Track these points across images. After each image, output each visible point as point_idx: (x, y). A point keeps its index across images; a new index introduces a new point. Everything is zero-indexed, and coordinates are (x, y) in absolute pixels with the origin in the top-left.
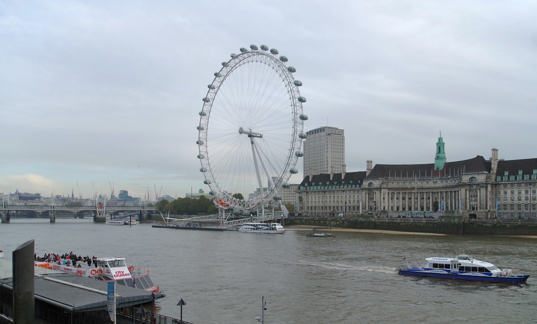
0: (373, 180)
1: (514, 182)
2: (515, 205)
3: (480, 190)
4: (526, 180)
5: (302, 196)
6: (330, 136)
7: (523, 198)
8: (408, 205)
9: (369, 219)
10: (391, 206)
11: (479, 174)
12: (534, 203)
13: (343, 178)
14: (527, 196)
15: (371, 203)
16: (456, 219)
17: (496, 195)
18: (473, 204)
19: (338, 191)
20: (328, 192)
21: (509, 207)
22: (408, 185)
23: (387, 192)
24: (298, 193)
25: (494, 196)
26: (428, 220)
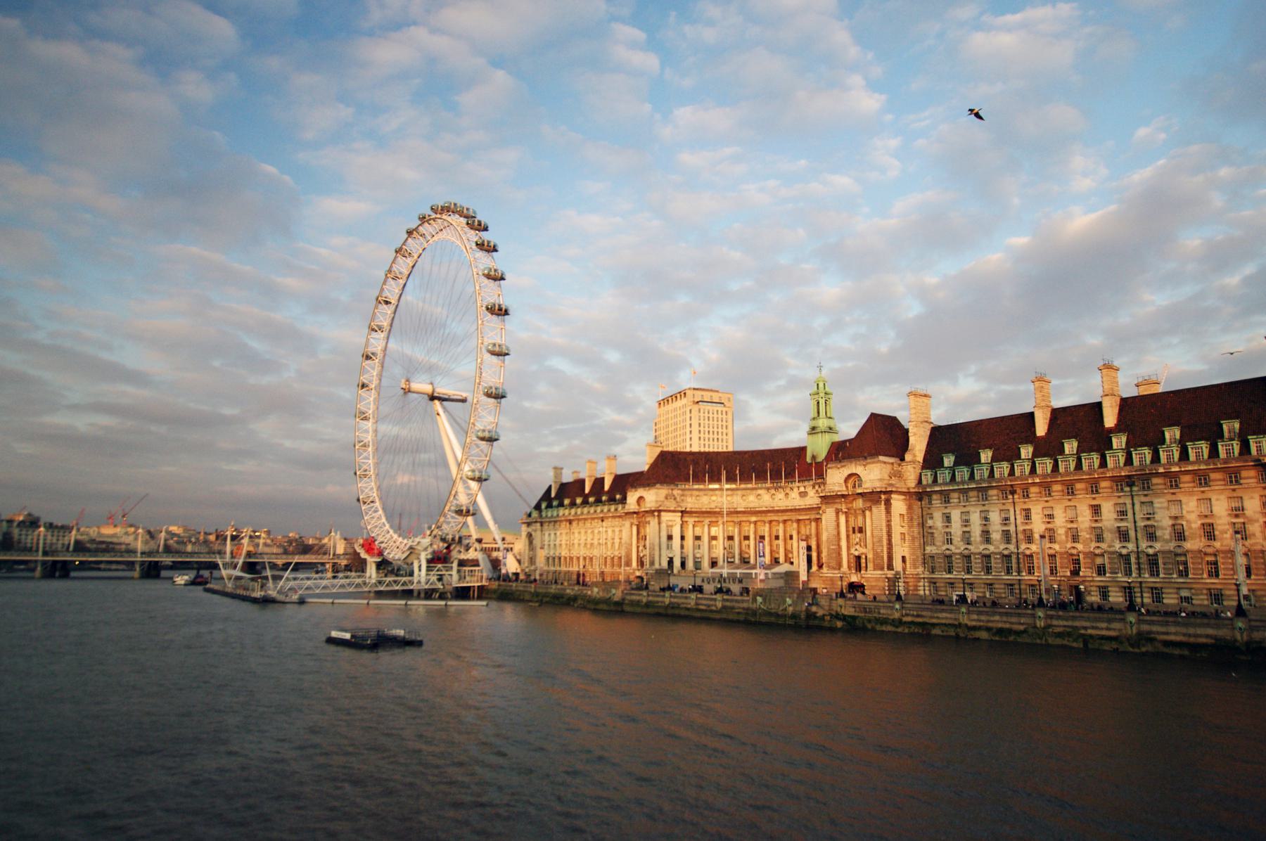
1: (966, 487)
2: (976, 559)
4: (999, 480)
6: (697, 405)
8: (741, 554)
9: (611, 592)
11: (870, 463)
12: (1028, 552)
13: (607, 487)
15: (641, 548)
16: (788, 599)
17: (923, 525)
18: (857, 553)
20: (576, 522)
21: (958, 563)
23: (678, 520)
25: (916, 530)
26: (727, 600)
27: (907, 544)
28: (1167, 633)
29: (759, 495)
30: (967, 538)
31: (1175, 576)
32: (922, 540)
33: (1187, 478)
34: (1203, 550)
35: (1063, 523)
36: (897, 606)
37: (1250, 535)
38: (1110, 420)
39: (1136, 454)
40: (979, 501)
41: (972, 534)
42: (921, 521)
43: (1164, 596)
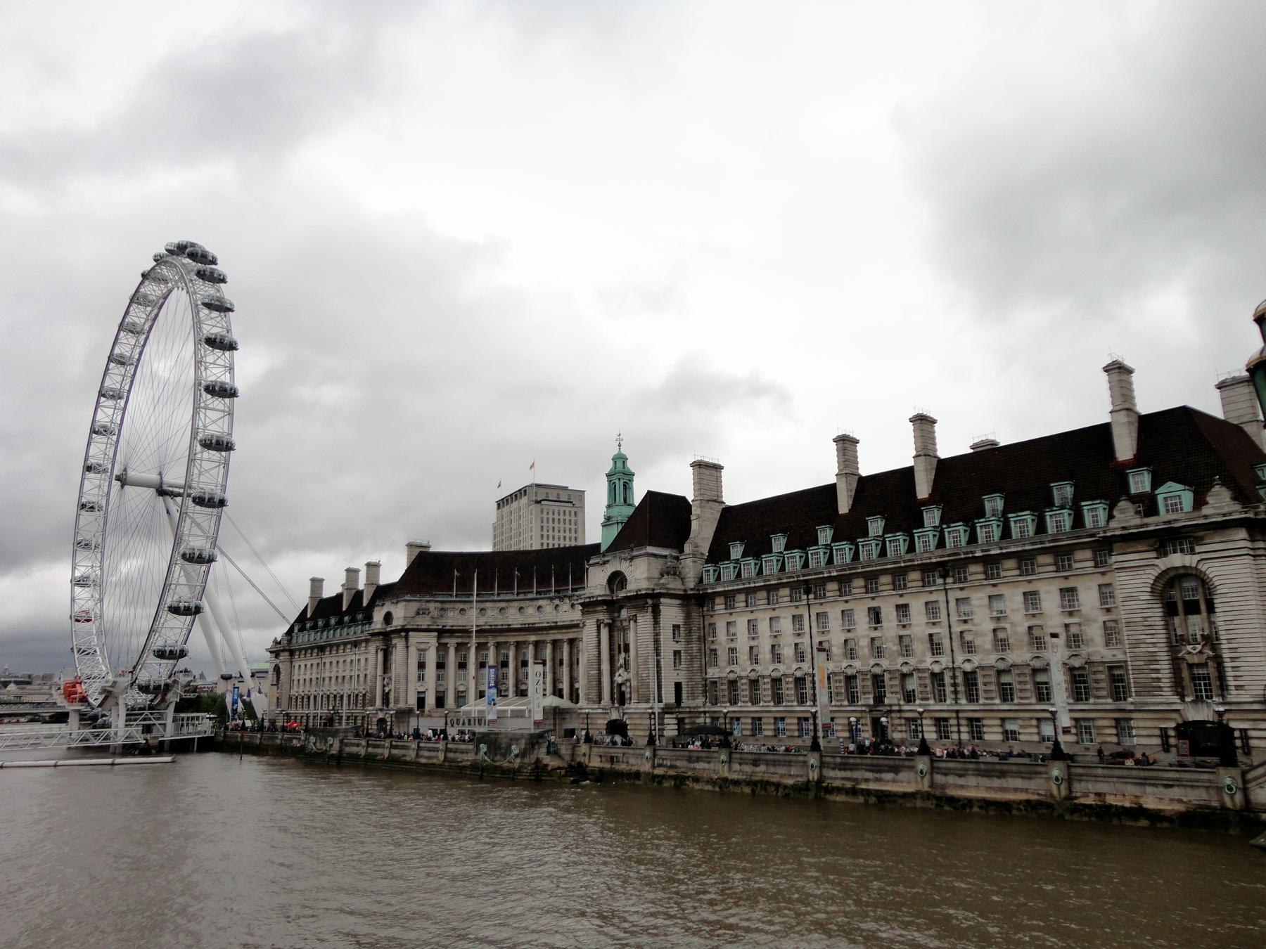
0: (393, 603)
1: (752, 585)
2: (764, 683)
3: (636, 621)
5: (281, 666)
6: (538, 505)
7: (788, 652)
10: (462, 692)
13: (365, 604)
14: (798, 641)
17: (703, 639)
19: (345, 644)
20: (328, 649)
22: (514, 617)
24: (274, 655)
25: (695, 646)
27: (683, 666)
28: (962, 787)
29: (540, 607)
30: (754, 658)
31: (997, 701)
32: (703, 660)
33: (1011, 563)
34: (1031, 663)
35: (866, 630)
36: (648, 753)
37: (1087, 641)
38: (923, 489)
39: (949, 532)
40: (768, 604)
41: (761, 650)
42: (702, 634)
43: (985, 729)
